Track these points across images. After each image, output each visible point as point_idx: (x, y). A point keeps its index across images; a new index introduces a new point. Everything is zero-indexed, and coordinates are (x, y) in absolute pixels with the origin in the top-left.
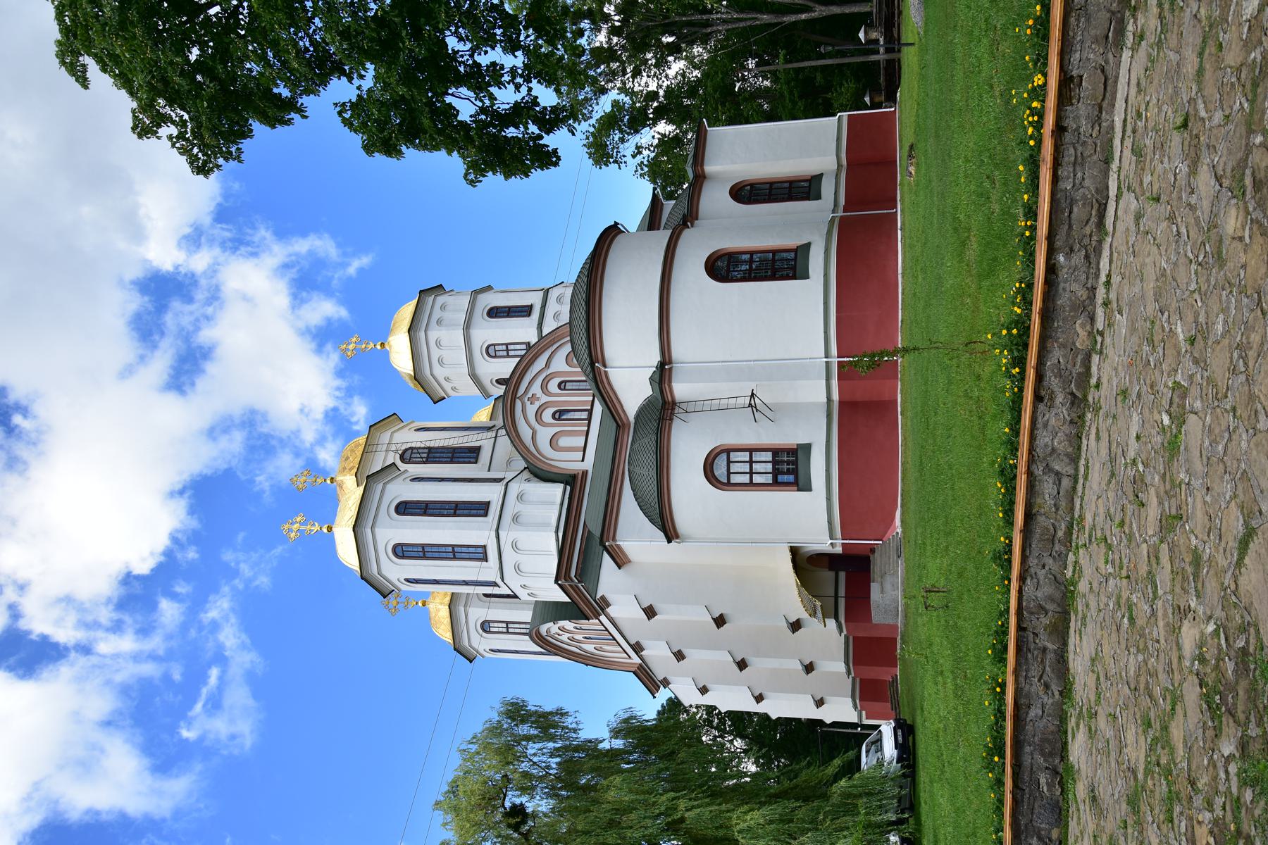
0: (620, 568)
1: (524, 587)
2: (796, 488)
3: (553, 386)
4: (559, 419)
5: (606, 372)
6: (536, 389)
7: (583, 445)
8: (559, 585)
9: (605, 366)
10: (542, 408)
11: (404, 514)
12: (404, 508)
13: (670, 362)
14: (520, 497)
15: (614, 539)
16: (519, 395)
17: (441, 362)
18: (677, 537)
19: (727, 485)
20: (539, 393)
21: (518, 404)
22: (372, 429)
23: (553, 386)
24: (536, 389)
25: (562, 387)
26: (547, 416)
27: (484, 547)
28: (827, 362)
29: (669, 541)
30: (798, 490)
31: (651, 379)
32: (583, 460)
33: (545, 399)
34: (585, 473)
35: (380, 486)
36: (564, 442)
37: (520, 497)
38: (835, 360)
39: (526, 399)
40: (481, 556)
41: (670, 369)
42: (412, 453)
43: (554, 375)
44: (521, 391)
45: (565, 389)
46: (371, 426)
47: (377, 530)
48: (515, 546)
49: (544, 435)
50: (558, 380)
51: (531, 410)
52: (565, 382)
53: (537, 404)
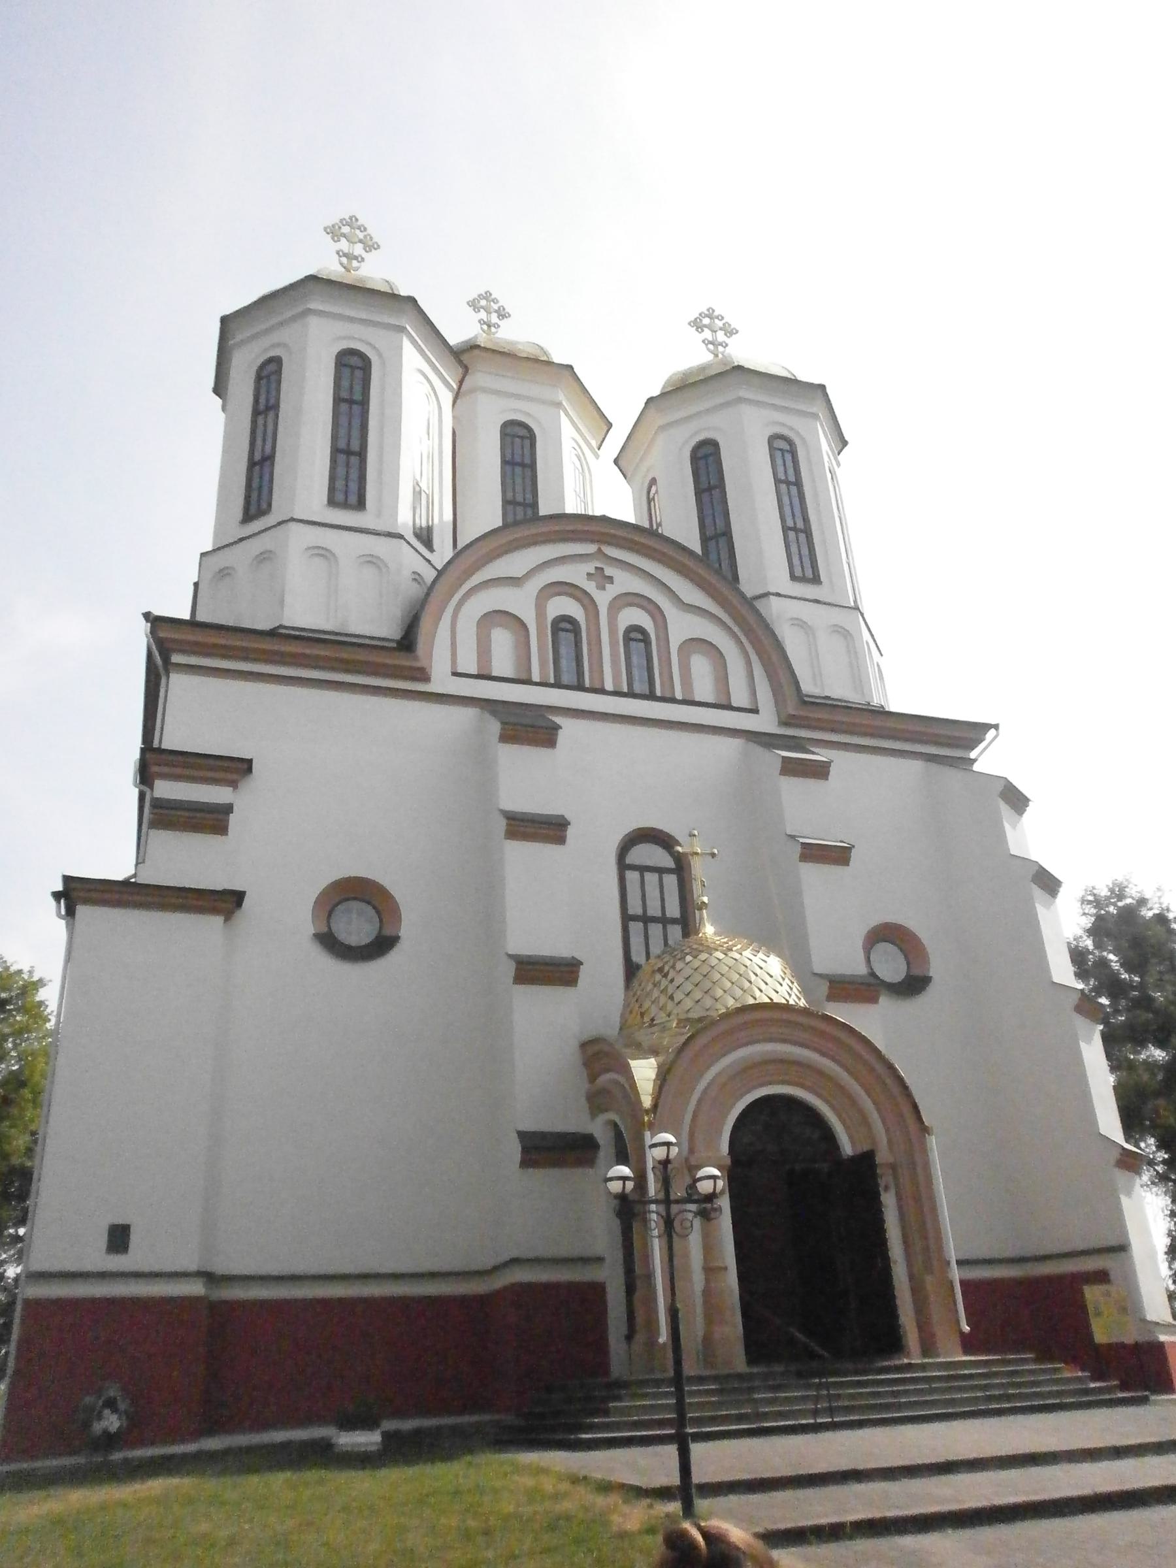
6: (625, 582)
7: (494, 674)
20: (612, 591)
21: (591, 548)
23: (633, 616)
24: (625, 582)
25: (633, 635)
32: (455, 674)
33: (603, 599)
34: (423, 675)
36: (502, 641)
42: (522, 438)
49: (521, 602)
50: (647, 623)
51: (576, 574)
52: (646, 640)
53: (590, 587)
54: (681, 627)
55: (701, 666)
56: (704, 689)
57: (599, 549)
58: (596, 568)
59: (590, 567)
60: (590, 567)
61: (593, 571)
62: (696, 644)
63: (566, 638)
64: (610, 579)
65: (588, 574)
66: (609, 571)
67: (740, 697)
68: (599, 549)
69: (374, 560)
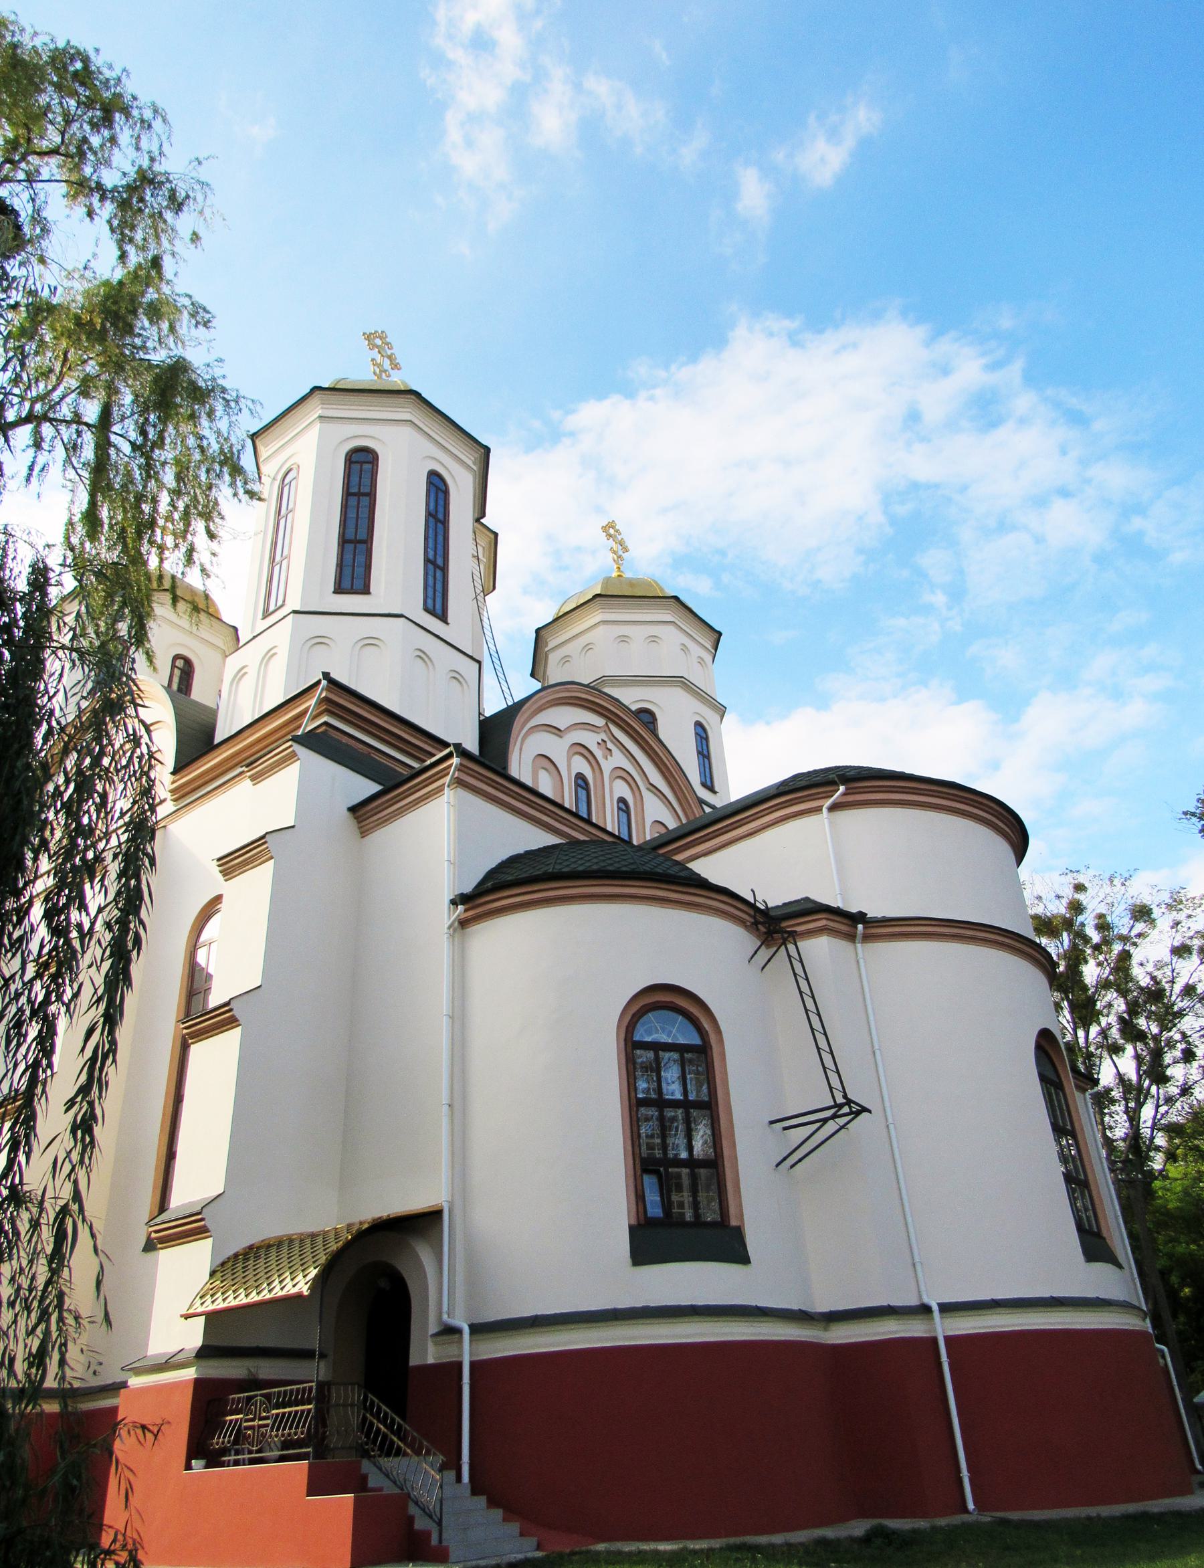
0: (353, 809)
1: (270, 655)
2: (634, 1222)
3: (621, 789)
4: (577, 785)
5: (818, 810)
6: (618, 759)
8: (319, 682)
9: (833, 808)
11: (430, 483)
12: (437, 486)
13: (866, 938)
14: (457, 677)
15: (460, 783)
16: (610, 725)
17: (623, 639)
18: (463, 923)
19: (631, 1046)
21: (599, 721)
22: (492, 536)
23: (621, 789)
26: (581, 765)
27: (366, 590)
28: (925, 1310)
29: (462, 899)
30: (631, 1228)
31: (807, 899)
33: (607, 766)
35: (470, 463)
37: (457, 677)
38: (943, 1328)
39: (606, 739)
40: (346, 584)
41: (851, 937)
46: (496, 535)
47: (407, 430)
48: (370, 642)
51: (590, 740)
53: (598, 753)
58: (603, 740)
59: (599, 737)
60: (599, 737)
61: (600, 742)
63: (582, 794)
64: (610, 750)
65: (599, 743)
66: (610, 745)
69: (457, 676)
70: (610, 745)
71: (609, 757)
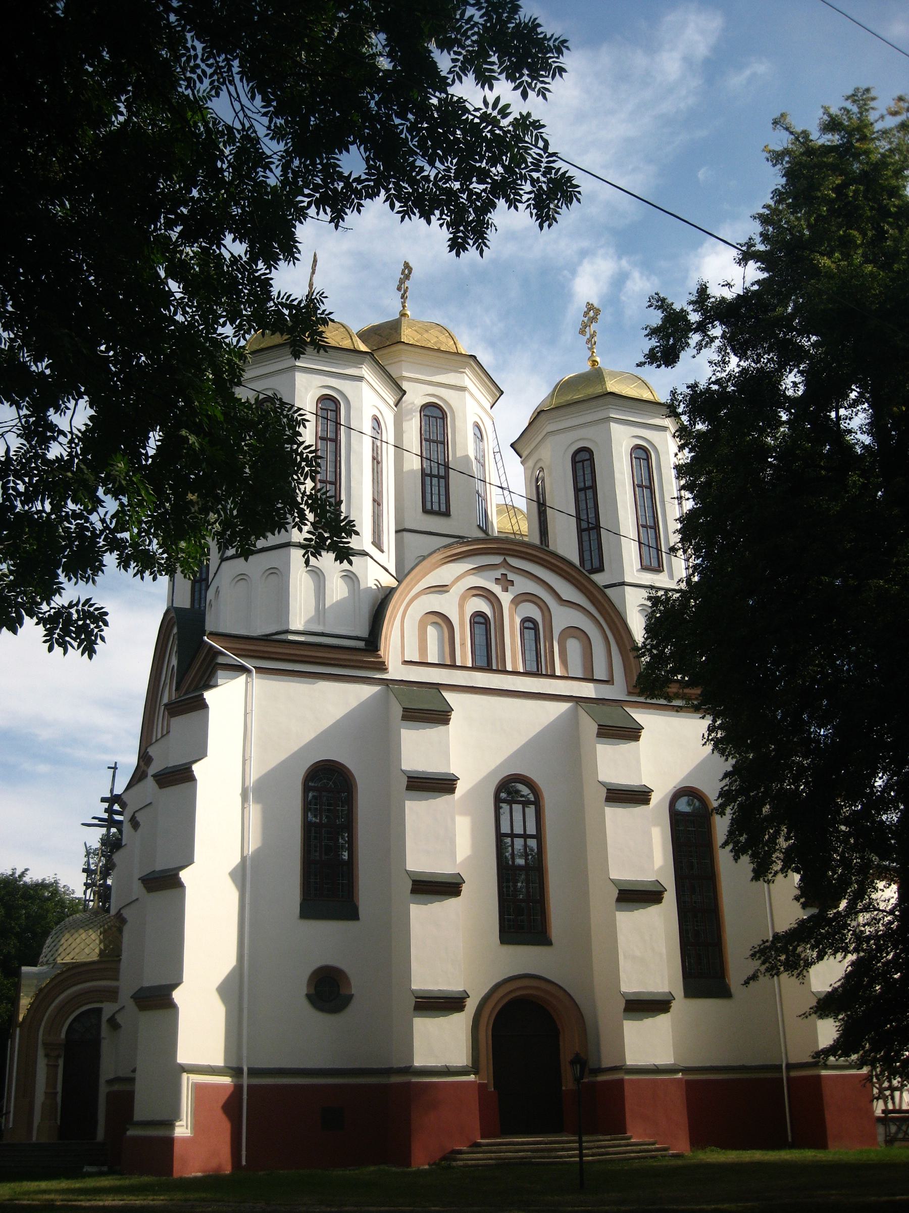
6: (523, 585)
10: (492, 599)
21: (498, 560)
33: (506, 598)
36: (432, 633)
43: (546, 614)
44: (514, 562)
45: (523, 628)
52: (536, 628)
53: (497, 589)
54: (563, 618)
55: (574, 646)
56: (576, 668)
57: (505, 559)
58: (502, 574)
59: (498, 574)
60: (498, 574)
62: (573, 631)
63: (479, 630)
64: (512, 581)
66: (511, 576)
67: (600, 672)
68: (505, 559)
70: (511, 576)
71: (510, 588)
